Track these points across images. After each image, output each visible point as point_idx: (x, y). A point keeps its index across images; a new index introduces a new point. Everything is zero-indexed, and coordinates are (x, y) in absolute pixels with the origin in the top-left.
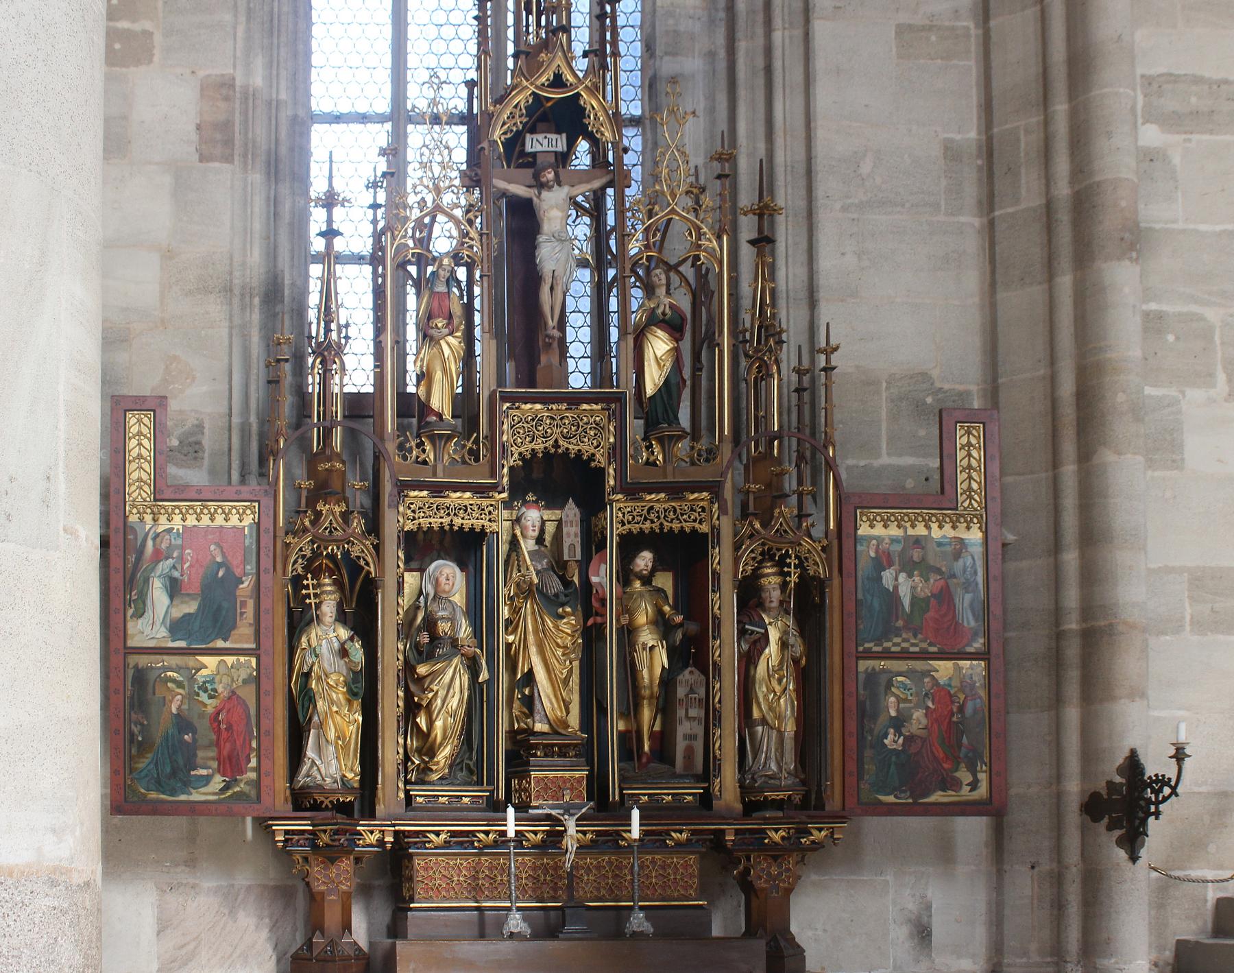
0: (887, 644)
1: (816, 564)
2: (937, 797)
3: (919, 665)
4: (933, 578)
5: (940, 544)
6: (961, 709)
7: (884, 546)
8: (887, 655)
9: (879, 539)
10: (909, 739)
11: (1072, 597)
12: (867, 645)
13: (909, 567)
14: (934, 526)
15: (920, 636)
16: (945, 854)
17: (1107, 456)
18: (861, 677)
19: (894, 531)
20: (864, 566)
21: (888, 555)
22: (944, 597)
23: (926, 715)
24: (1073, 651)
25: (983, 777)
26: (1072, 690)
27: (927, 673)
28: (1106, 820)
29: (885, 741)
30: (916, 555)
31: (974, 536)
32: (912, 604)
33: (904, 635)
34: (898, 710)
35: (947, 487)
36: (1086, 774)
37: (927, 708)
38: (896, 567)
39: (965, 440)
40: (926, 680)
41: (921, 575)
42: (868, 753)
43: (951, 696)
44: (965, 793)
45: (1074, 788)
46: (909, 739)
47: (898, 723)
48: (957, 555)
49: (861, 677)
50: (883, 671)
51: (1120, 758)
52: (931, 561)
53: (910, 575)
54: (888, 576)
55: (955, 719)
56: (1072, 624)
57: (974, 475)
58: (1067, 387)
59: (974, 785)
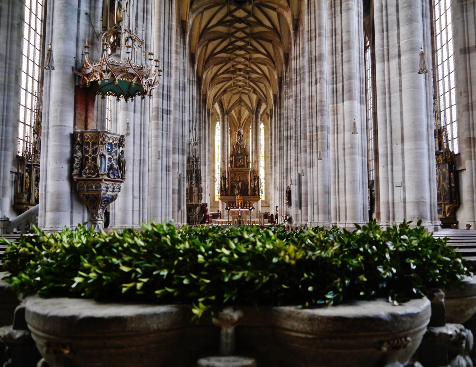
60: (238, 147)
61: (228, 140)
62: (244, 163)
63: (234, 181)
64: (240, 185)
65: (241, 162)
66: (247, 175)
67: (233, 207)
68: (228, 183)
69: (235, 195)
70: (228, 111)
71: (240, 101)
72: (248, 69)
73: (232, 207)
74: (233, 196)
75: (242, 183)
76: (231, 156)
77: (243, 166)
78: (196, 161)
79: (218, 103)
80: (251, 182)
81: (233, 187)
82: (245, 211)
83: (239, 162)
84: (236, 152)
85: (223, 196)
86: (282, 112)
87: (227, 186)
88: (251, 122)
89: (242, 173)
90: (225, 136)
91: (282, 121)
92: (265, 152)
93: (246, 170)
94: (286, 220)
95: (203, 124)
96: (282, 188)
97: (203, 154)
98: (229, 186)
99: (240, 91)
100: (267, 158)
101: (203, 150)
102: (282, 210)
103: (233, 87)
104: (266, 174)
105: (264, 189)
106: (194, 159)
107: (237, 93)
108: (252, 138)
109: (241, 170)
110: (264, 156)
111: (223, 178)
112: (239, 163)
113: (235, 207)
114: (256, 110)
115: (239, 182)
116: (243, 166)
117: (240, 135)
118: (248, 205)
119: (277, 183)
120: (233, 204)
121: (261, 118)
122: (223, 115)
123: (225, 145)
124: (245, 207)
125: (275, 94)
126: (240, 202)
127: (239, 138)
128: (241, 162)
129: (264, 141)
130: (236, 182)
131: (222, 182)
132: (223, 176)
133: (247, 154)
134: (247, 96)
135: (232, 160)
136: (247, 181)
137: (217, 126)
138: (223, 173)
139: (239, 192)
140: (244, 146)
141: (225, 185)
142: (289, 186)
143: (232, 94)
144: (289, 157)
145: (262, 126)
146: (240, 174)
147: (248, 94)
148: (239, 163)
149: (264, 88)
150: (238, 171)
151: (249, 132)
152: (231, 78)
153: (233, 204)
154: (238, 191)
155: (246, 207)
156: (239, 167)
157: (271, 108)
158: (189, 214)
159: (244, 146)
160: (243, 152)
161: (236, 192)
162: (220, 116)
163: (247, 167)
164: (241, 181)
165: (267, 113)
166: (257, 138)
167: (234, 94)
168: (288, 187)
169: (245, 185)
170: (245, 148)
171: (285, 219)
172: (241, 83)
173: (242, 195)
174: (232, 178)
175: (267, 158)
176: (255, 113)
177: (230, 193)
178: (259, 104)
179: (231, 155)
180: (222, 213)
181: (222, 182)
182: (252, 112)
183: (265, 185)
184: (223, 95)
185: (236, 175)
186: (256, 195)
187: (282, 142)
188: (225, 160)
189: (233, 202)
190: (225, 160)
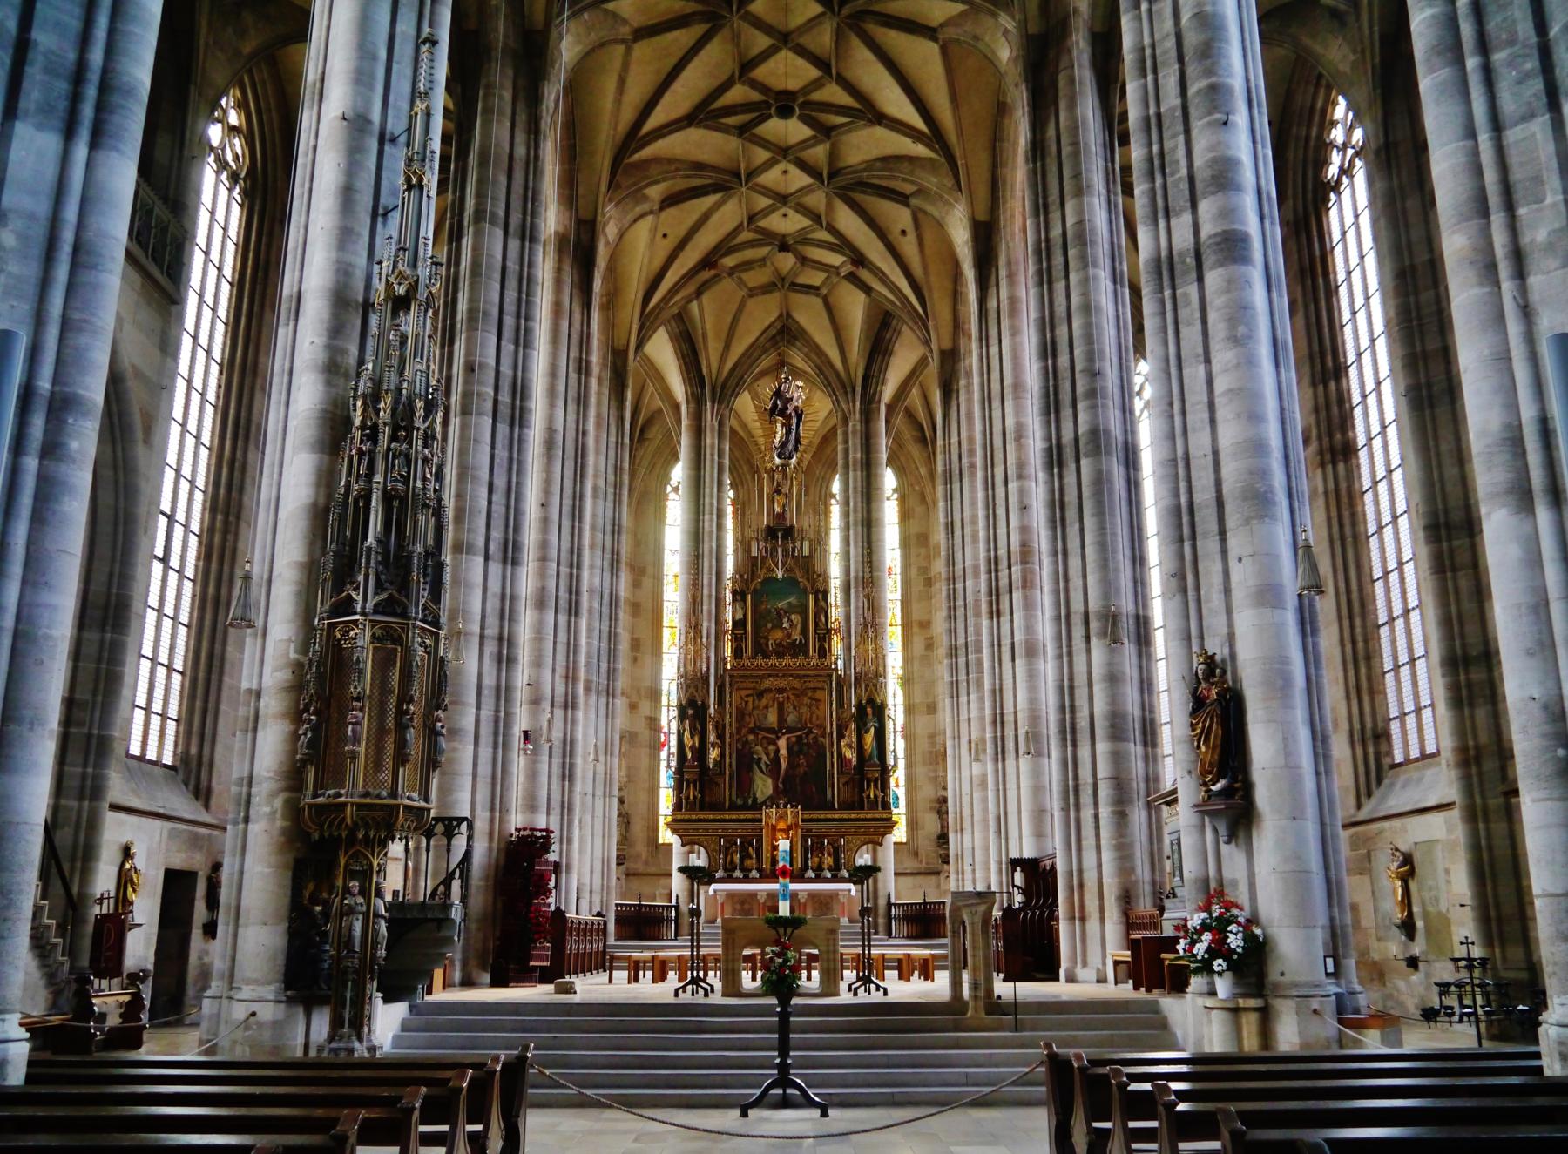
60: (774, 550)
61: (720, 527)
62: (804, 631)
63: (752, 731)
64: (783, 752)
65: (791, 626)
66: (819, 694)
67: (746, 870)
68: (721, 737)
69: (757, 807)
70: (724, 386)
71: (786, 332)
72: (834, 93)
73: (738, 874)
74: (745, 807)
75: (793, 737)
76: (738, 596)
77: (798, 649)
78: (402, 423)
79: (674, 339)
80: (841, 736)
81: (746, 763)
82: (812, 895)
83: (779, 626)
84: (762, 575)
85: (691, 807)
86: (1056, 232)
87: (713, 754)
88: (840, 462)
89: (796, 683)
90: (709, 500)
91: (1060, 287)
92: (905, 603)
93: (816, 668)
94: (1219, 964)
95: (573, 376)
96: (1083, 723)
97: (565, 545)
98: (722, 755)
99: (783, 279)
100: (916, 629)
101: (566, 523)
102: (1090, 877)
103: (751, 244)
104: (909, 710)
105: (902, 782)
106: (385, 404)
107: (767, 289)
108: (846, 515)
109: (788, 668)
110: (899, 622)
111: (692, 711)
112: (779, 635)
113: (754, 874)
114: (866, 379)
115: (777, 733)
116: (798, 649)
117: (783, 413)
118: (828, 860)
119: (1009, 718)
120: (745, 856)
121: (887, 422)
122: (697, 399)
123: (708, 546)
124: (810, 874)
125: (982, 216)
126: (784, 844)
127: (780, 431)
128: (791, 626)
129: (898, 553)
130: (762, 734)
131: (687, 736)
132: (692, 702)
133: (820, 585)
134: (818, 302)
135: (739, 616)
136: (822, 727)
137: (674, 482)
138: (693, 683)
139: (776, 788)
140: (806, 544)
141: (701, 753)
142: (1216, 647)
143: (744, 292)
144: (1198, 416)
145: (889, 480)
146: (781, 690)
147: (824, 291)
148: (779, 635)
149: (911, 237)
150: (774, 673)
151: (827, 513)
152: (738, 175)
153: (745, 856)
154: (770, 781)
155: (819, 869)
156: (780, 655)
157: (947, 345)
158: (315, 900)
159: (806, 544)
160: (799, 575)
161: (763, 786)
162: (684, 408)
163: (824, 652)
164: (790, 730)
165: (910, 415)
166: (869, 511)
167: (753, 292)
168: (1210, 661)
169: (809, 750)
170: (810, 556)
171: (1213, 953)
172: (788, 223)
173: (793, 801)
174: (741, 715)
175: (916, 629)
176: (859, 389)
177: (727, 792)
178: (879, 348)
179: (734, 593)
180: (684, 908)
181: (687, 736)
182: (844, 387)
183: (910, 765)
184: (699, 293)
185: (760, 695)
186: (873, 805)
187: (1067, 412)
188: (707, 625)
189: (746, 843)
190: (707, 625)
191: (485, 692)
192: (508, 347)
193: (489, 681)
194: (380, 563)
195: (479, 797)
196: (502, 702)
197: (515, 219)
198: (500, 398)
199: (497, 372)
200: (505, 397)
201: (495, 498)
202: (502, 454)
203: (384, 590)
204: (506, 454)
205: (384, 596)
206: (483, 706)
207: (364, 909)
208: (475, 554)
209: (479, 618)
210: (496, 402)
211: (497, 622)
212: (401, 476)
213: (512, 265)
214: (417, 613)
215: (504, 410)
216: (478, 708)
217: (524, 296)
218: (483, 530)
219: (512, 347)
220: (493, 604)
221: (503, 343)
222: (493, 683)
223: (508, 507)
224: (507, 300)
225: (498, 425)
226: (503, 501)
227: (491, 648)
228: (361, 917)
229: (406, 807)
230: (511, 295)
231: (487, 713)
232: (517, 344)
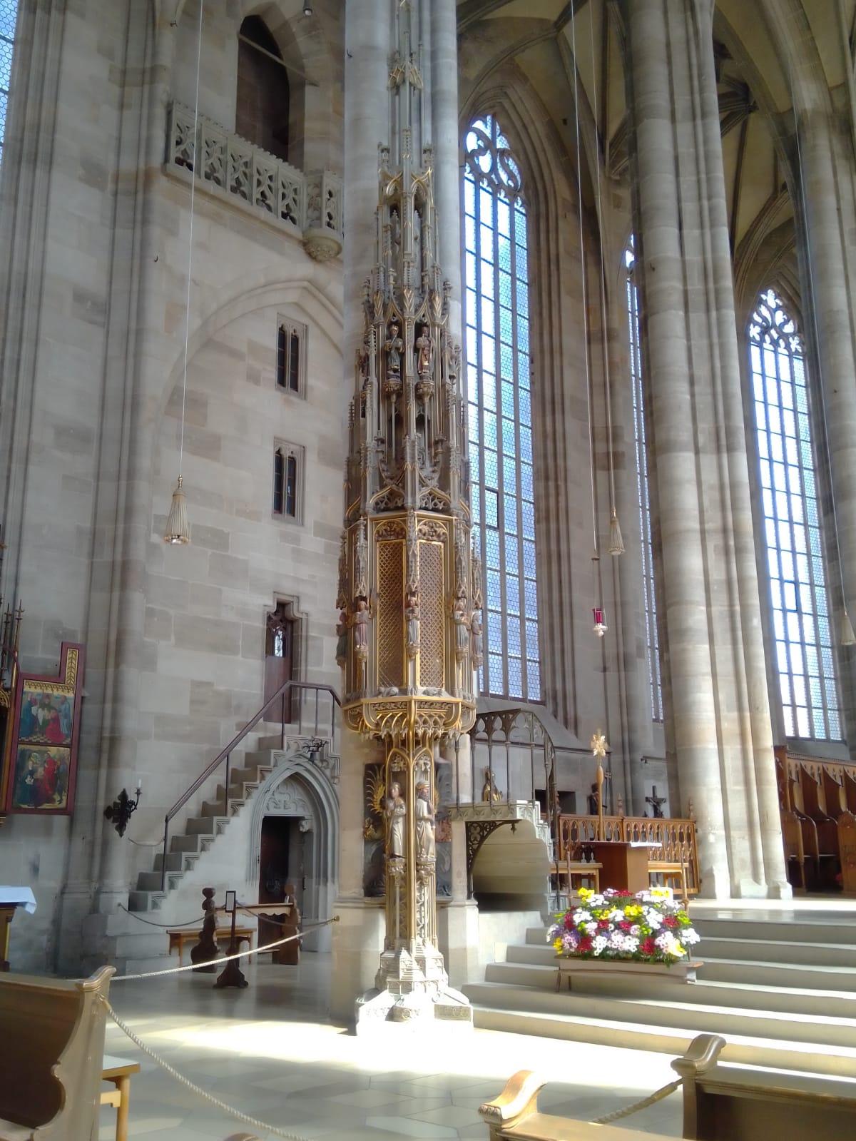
0: (30, 738)
1: (5, 701)
2: (46, 806)
3: (43, 748)
4: (52, 711)
5: (56, 698)
6: (58, 768)
7: (34, 697)
8: (30, 743)
9: (32, 693)
10: (36, 780)
11: (107, 723)
12: (23, 738)
13: (43, 706)
14: (55, 690)
15: (45, 736)
16: (48, 831)
17: (124, 667)
18: (19, 752)
19: (39, 690)
20: (25, 703)
21: (35, 700)
22: (56, 720)
23: (44, 770)
24: (106, 745)
25: (64, 798)
26: (104, 762)
27: (46, 752)
28: (112, 819)
29: (26, 781)
30: (47, 701)
31: (71, 695)
32: (43, 722)
33: (39, 735)
34: (33, 767)
35: (61, 674)
36: (107, 799)
37: (45, 767)
38: (38, 706)
39: (71, 656)
40: (46, 755)
41: (48, 710)
42: (18, 786)
43: (54, 762)
44: (57, 805)
45: (102, 805)
46: (36, 780)
47: (32, 773)
48: (63, 703)
49: (19, 752)
50: (28, 750)
51: (119, 793)
52: (52, 704)
53: (43, 709)
54: (34, 710)
55: (55, 772)
56: (107, 734)
57: (73, 670)
58: (113, 637)
59: (60, 802)
191: (714, 587)
192: (692, 233)
193: (717, 575)
194: (382, 461)
195: (721, 697)
196: (736, 595)
197: (682, 103)
198: (689, 288)
199: (684, 262)
200: (696, 285)
201: (697, 389)
202: (700, 343)
203: (382, 487)
204: (705, 342)
205: (385, 492)
206: (713, 602)
207: (404, 811)
208: (681, 450)
209: (696, 513)
210: (686, 293)
211: (718, 515)
212: (395, 371)
213: (686, 150)
214: (414, 502)
215: (697, 299)
216: (709, 605)
217: (703, 176)
218: (689, 424)
219: (697, 232)
220: (711, 496)
221: (685, 232)
222: (723, 576)
223: (714, 395)
224: (684, 187)
225: (692, 315)
226: (709, 390)
227: (714, 542)
228: (401, 820)
229: (421, 702)
230: (688, 180)
231: (720, 608)
232: (702, 226)
